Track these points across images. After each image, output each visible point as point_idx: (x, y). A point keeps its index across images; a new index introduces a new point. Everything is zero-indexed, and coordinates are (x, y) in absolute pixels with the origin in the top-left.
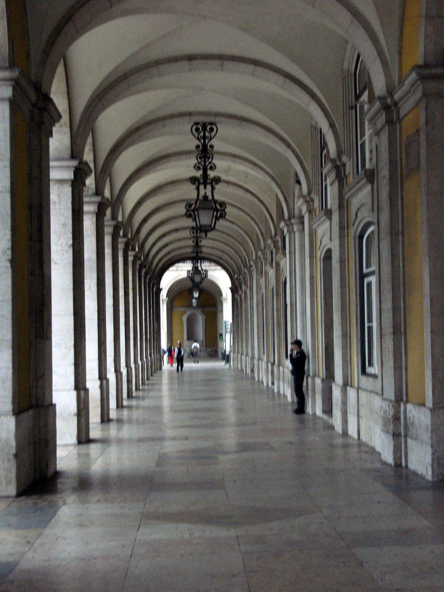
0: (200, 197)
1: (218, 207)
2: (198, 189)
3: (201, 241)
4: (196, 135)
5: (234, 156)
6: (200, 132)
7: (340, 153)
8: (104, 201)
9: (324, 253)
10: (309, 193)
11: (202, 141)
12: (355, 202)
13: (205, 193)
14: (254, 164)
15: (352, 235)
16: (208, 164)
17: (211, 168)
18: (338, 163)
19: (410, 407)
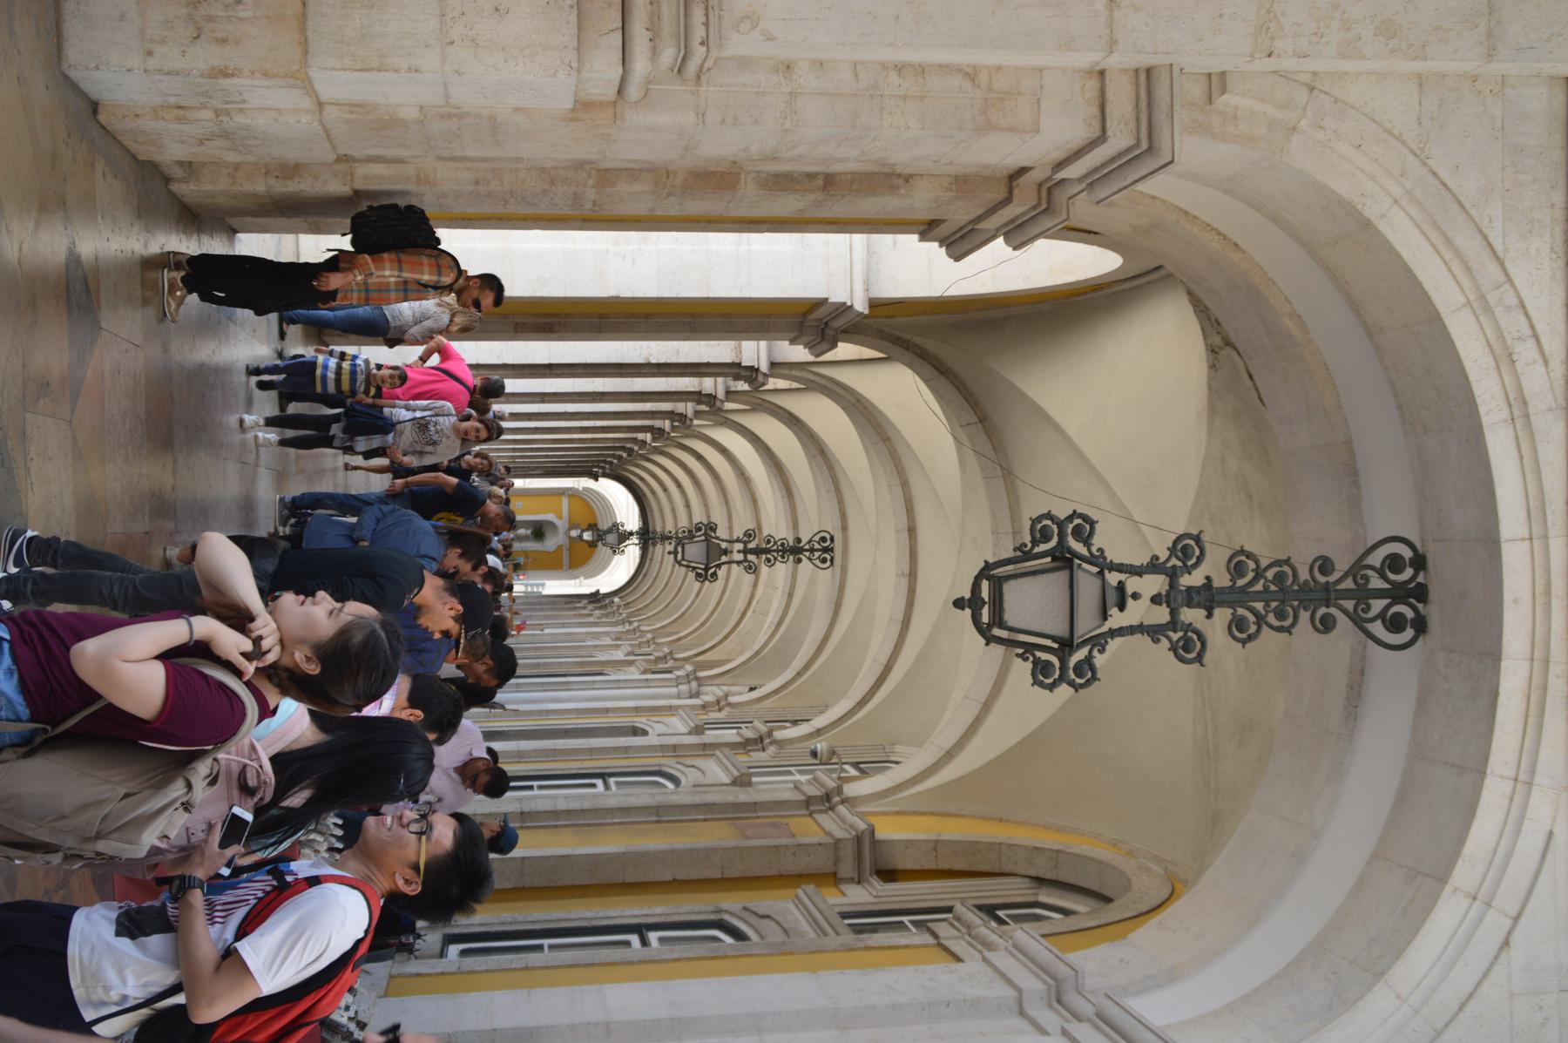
0: (1113, 578)
1: (1081, 654)
2: (1154, 566)
4: (1376, 559)
6: (1383, 577)
11: (1348, 584)
17: (1238, 624)
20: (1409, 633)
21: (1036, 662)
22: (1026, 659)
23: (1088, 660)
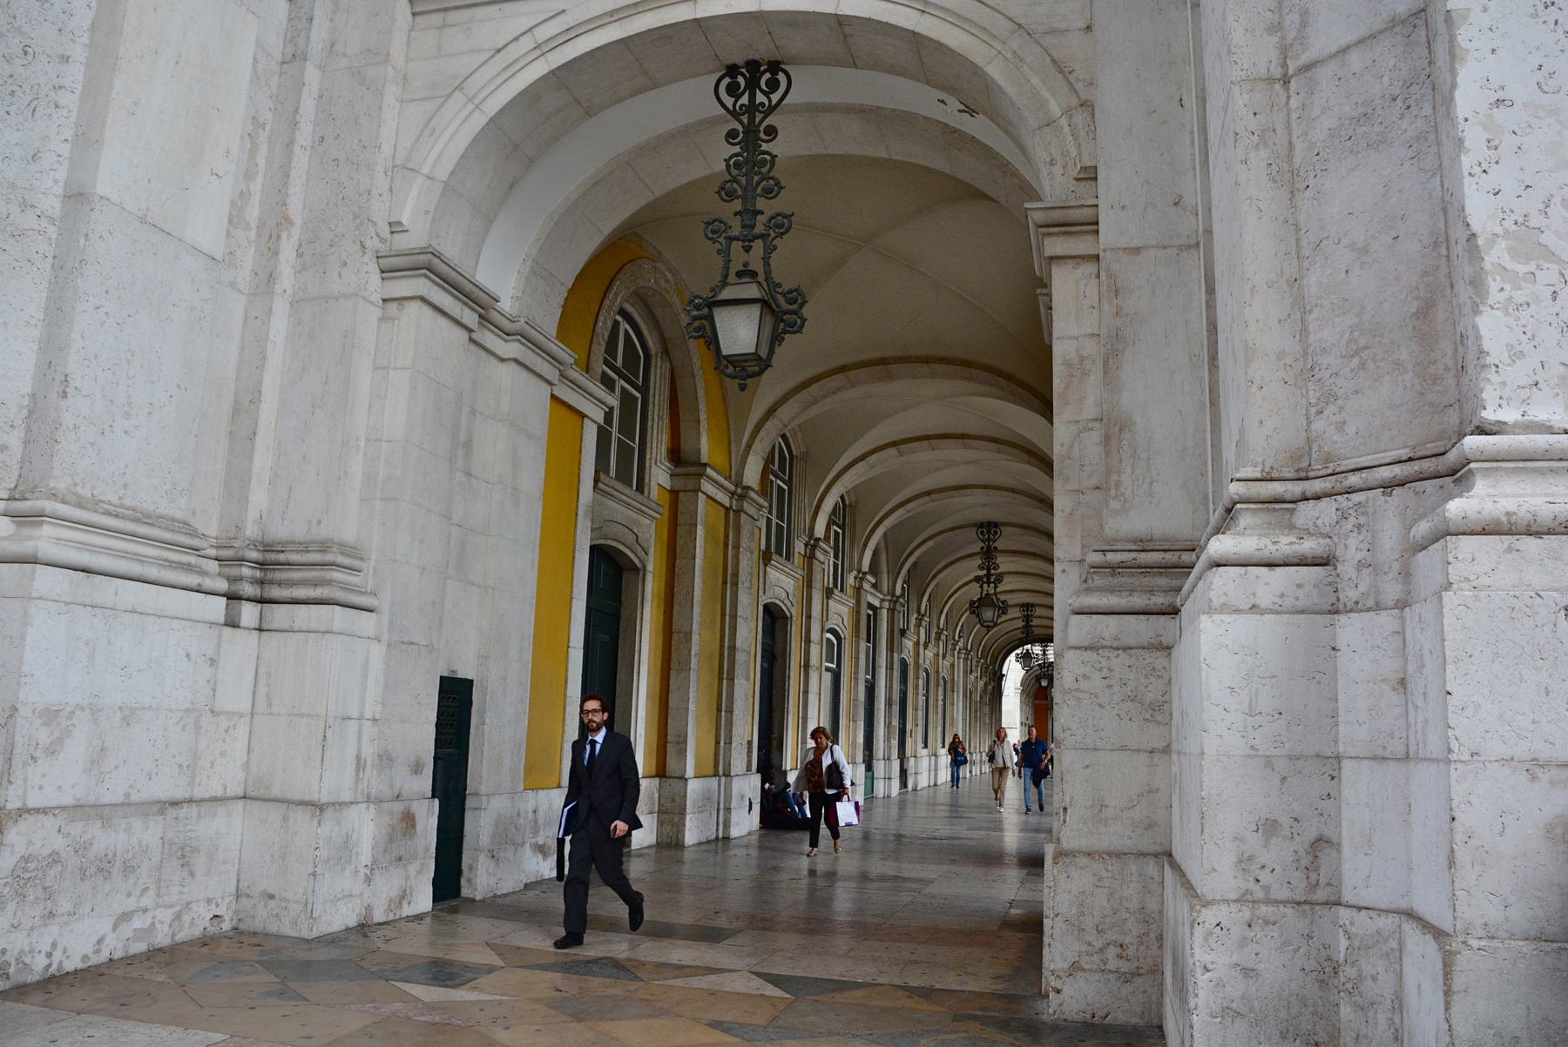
0: (732, 278)
1: (781, 299)
2: (725, 253)
4: (729, 101)
11: (745, 119)
16: (758, 183)
17: (769, 193)
20: (781, 77)
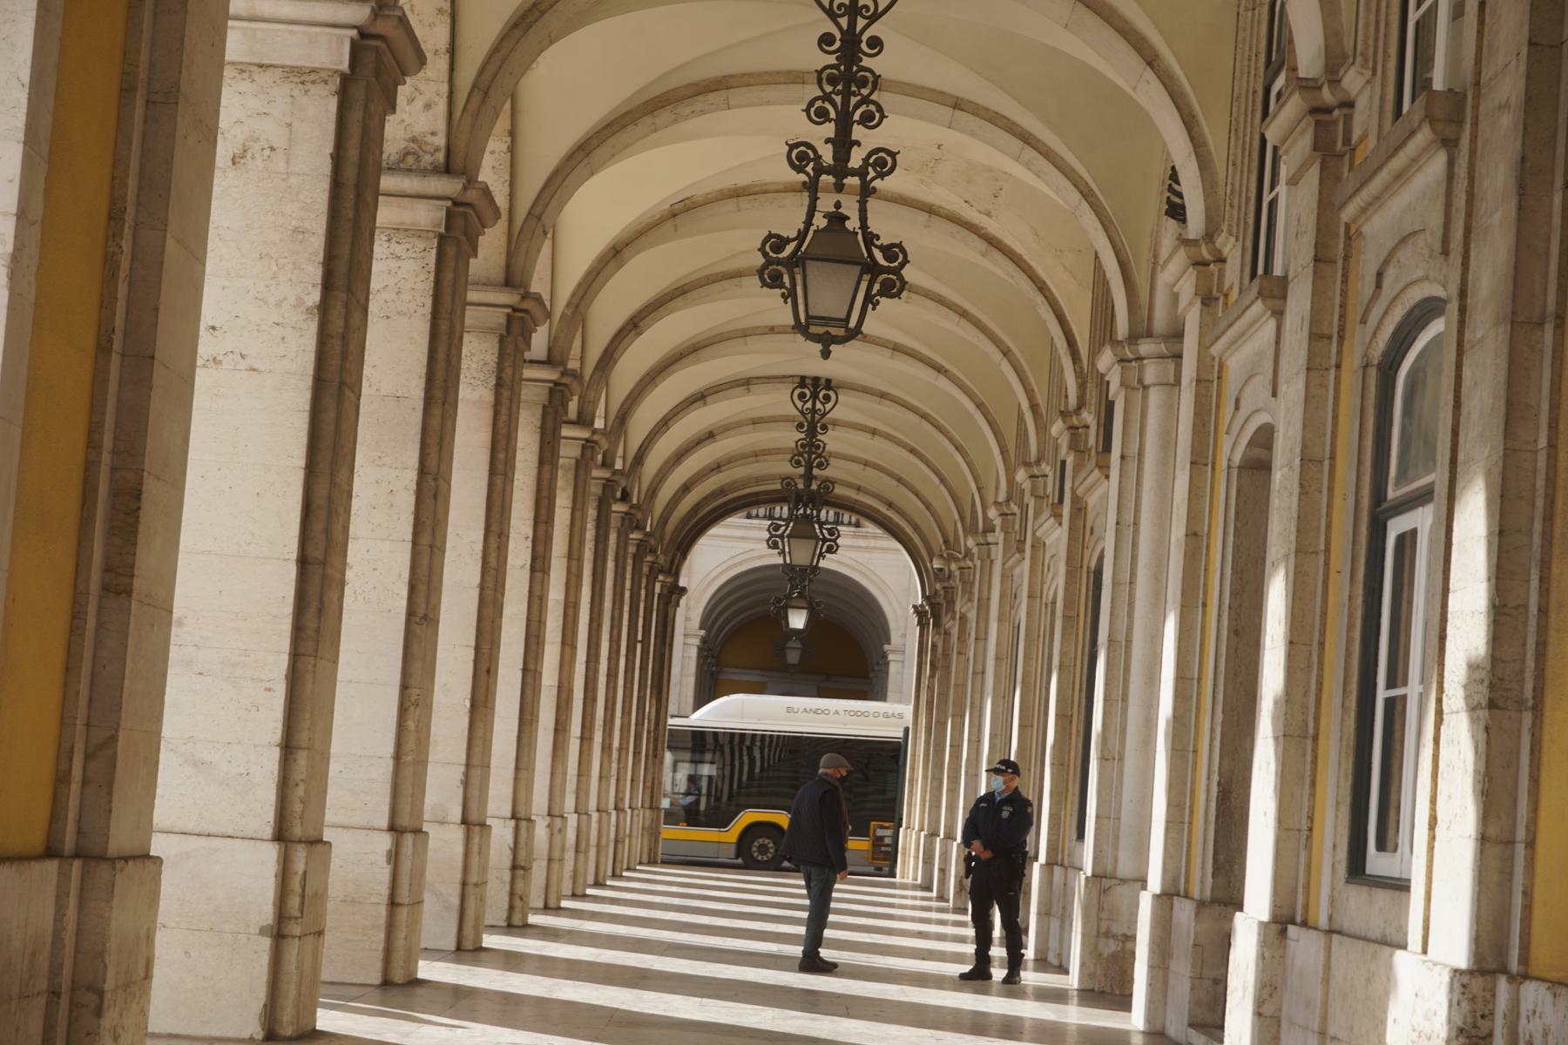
2: (812, 188)
3: (824, 427)
5: (958, 104)
7: (1334, 63)
8: (472, 195)
9: (1244, 440)
10: (1209, 236)
11: (844, 22)
12: (1378, 230)
13: (838, 205)
14: (1026, 138)
15: (1352, 361)
16: (857, 106)
17: (866, 120)
18: (1327, 96)
19: (1532, 993)
21: (880, 293)
22: (878, 302)
23: (888, 250)
